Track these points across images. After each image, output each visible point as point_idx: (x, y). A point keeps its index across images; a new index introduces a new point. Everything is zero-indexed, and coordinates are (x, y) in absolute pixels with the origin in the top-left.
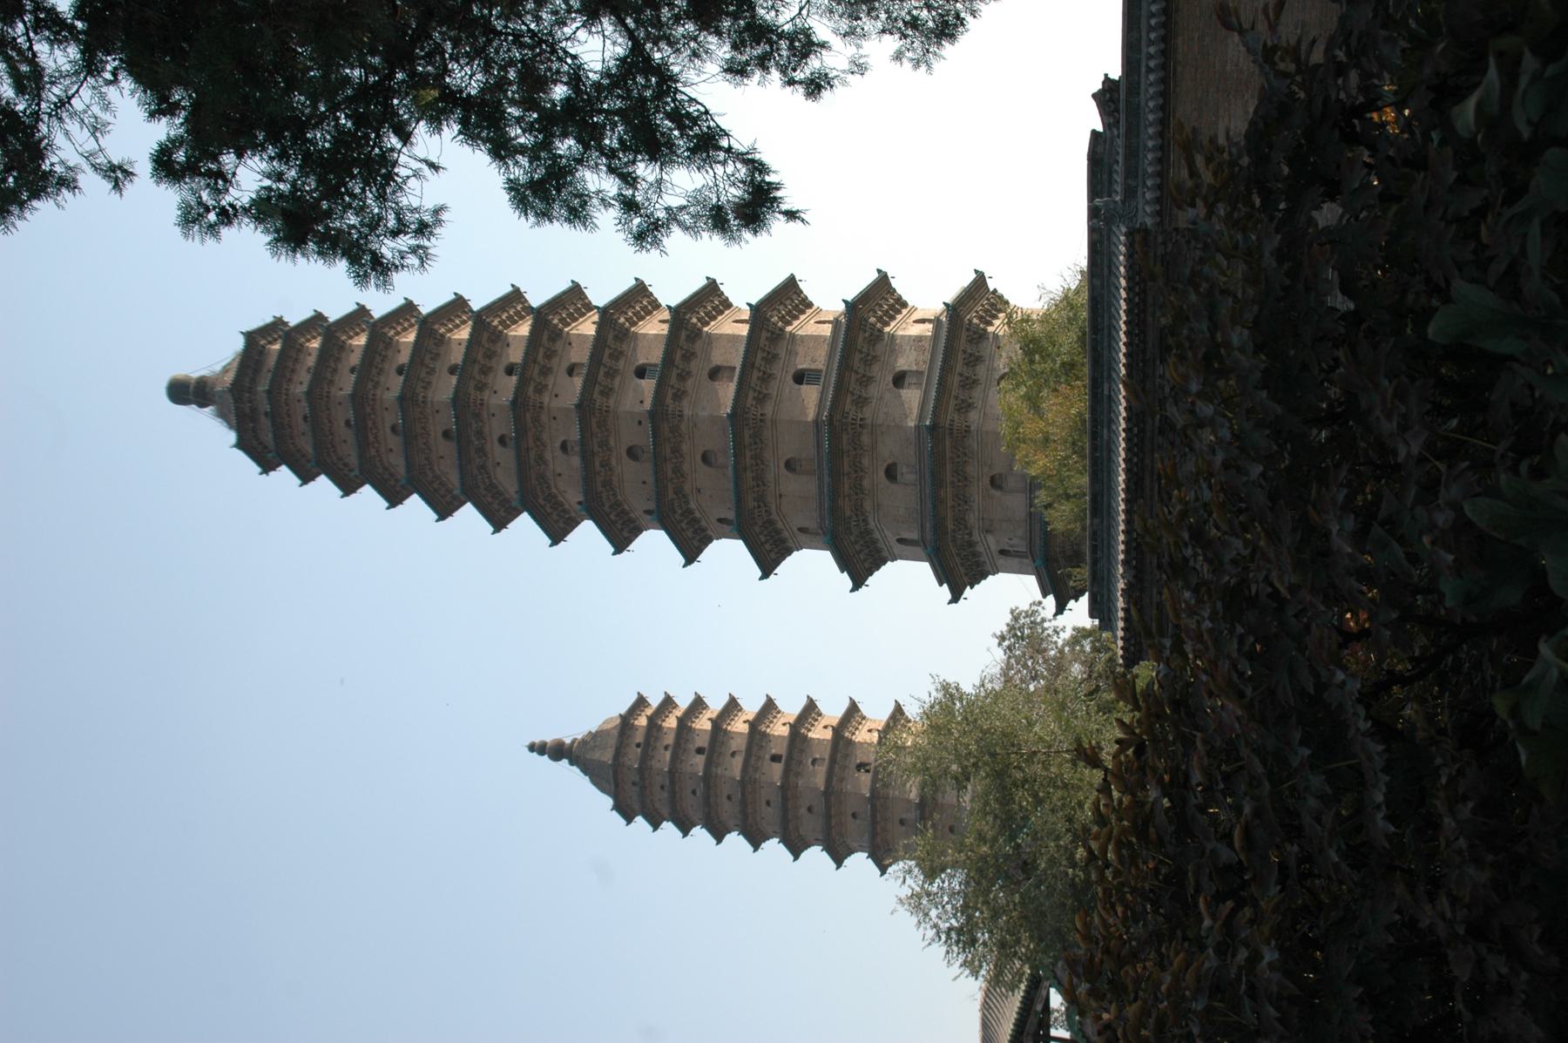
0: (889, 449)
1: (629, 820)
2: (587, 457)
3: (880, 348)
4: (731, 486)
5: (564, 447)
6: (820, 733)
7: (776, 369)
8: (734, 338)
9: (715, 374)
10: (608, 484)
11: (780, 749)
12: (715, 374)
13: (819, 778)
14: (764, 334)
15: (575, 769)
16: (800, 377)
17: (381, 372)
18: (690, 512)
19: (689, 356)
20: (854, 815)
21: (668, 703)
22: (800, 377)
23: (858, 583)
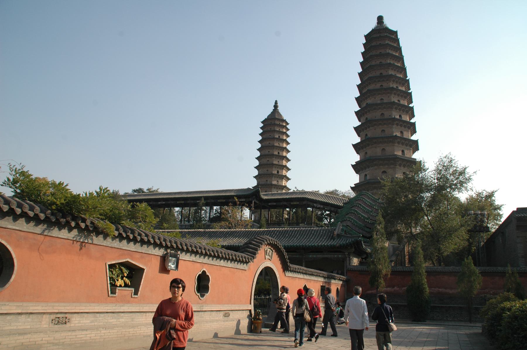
1: (262, 122)
5: (382, 99)
6: (284, 163)
7: (404, 146)
9: (402, 132)
11: (281, 154)
12: (402, 132)
13: (275, 162)
16: (403, 151)
17: (393, 60)
21: (288, 130)
22: (403, 151)
23: (353, 166)
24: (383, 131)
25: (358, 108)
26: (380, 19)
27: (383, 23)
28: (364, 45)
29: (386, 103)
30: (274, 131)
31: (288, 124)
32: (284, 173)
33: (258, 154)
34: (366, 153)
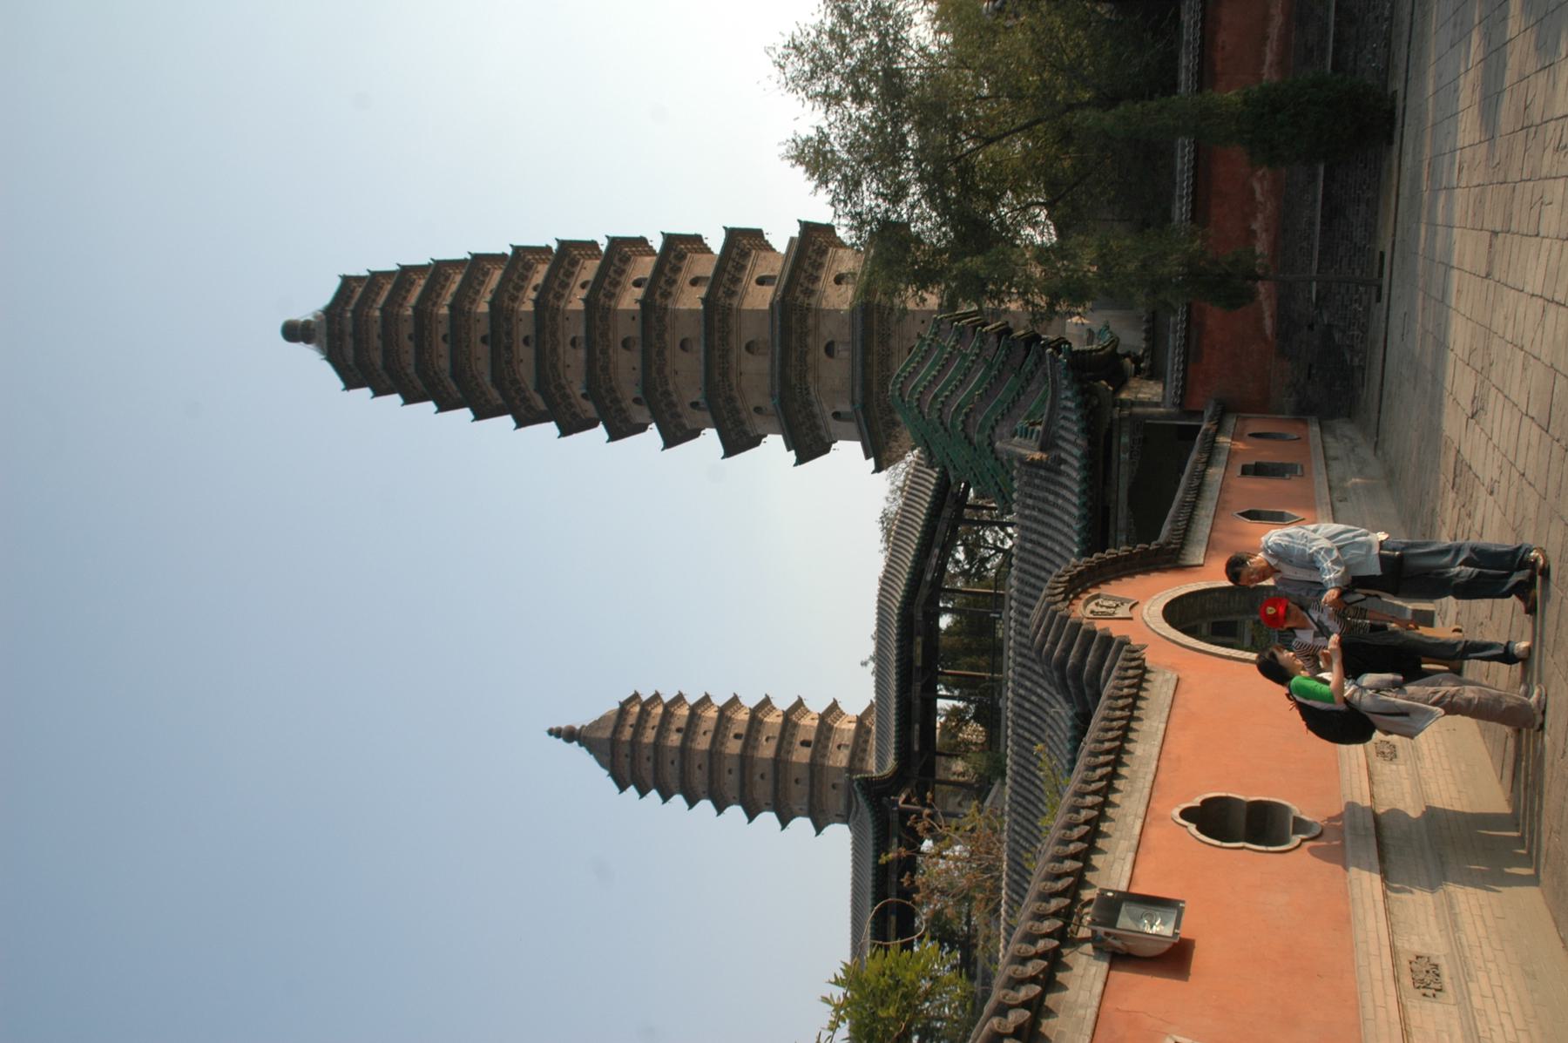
0: (828, 330)
4: (702, 368)
5: (573, 343)
6: (774, 720)
10: (605, 369)
11: (742, 730)
14: (735, 251)
15: (583, 749)
17: (439, 295)
18: (667, 393)
20: (797, 781)
22: (761, 281)
23: (801, 460)
24: (684, 345)
25: (600, 431)
26: (294, 332)
27: (307, 324)
28: (378, 393)
29: (589, 329)
30: (656, 750)
31: (636, 696)
32: (809, 723)
33: (735, 812)
34: (758, 410)
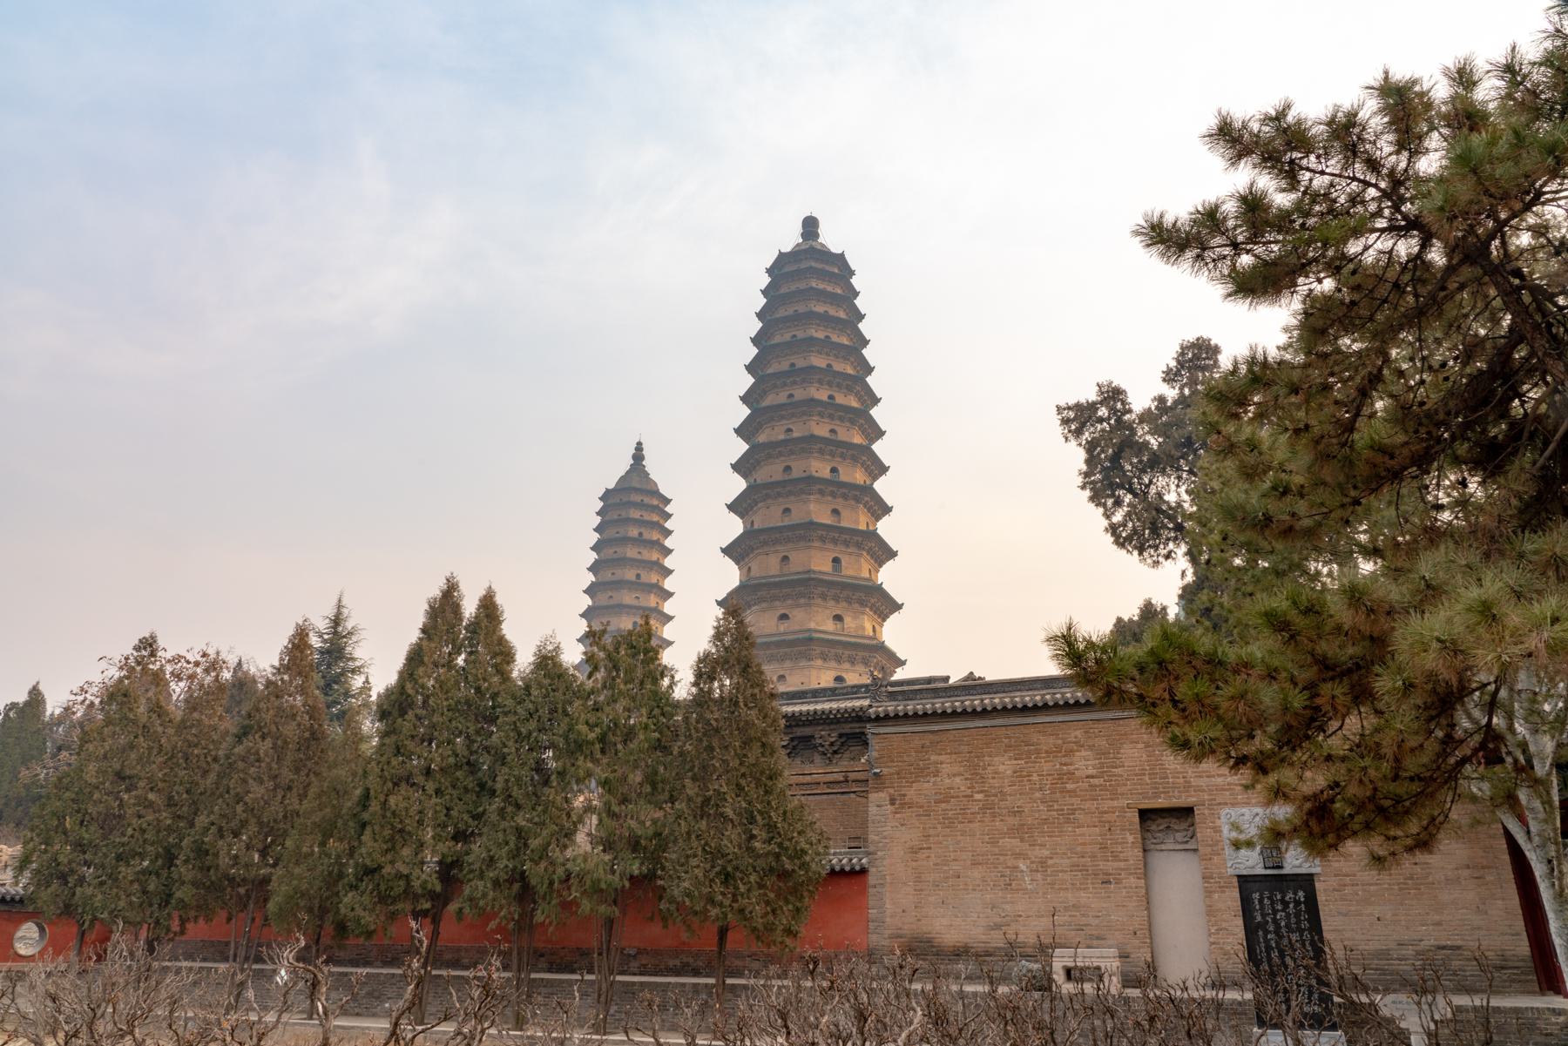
2: (784, 442)
3: (856, 606)
5: (790, 430)
8: (857, 522)
9: (835, 512)
10: (769, 456)
19: (845, 497)
22: (836, 561)
24: (787, 510)
26: (810, 226)
27: (817, 236)
31: (667, 501)
